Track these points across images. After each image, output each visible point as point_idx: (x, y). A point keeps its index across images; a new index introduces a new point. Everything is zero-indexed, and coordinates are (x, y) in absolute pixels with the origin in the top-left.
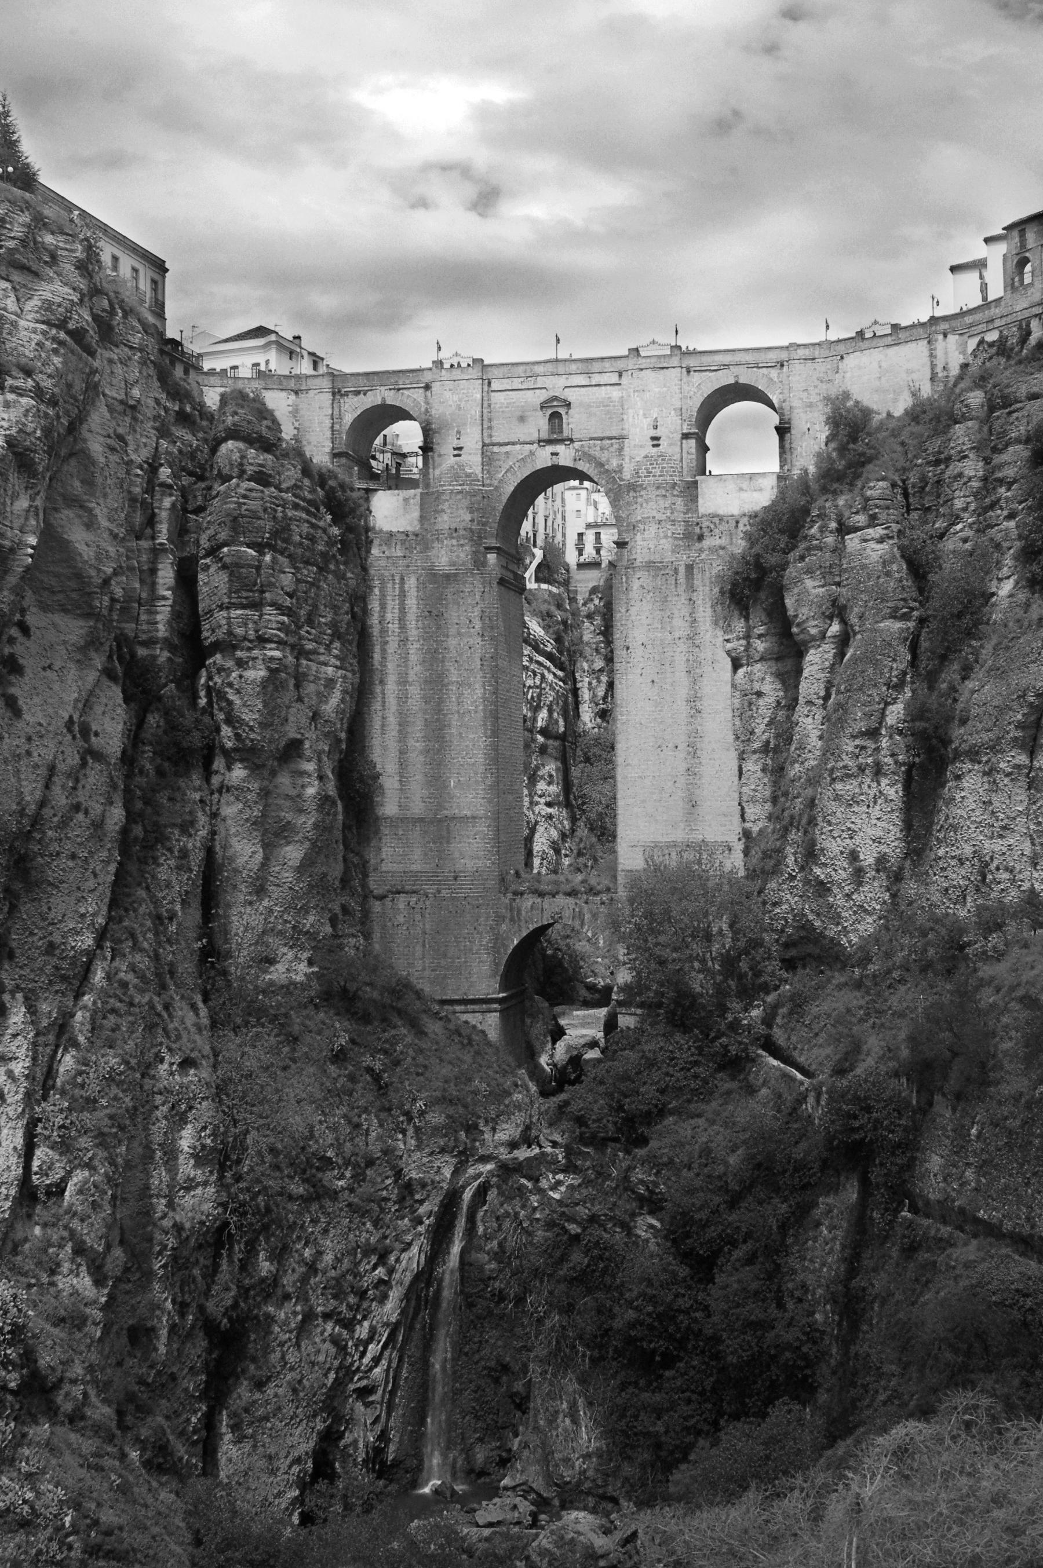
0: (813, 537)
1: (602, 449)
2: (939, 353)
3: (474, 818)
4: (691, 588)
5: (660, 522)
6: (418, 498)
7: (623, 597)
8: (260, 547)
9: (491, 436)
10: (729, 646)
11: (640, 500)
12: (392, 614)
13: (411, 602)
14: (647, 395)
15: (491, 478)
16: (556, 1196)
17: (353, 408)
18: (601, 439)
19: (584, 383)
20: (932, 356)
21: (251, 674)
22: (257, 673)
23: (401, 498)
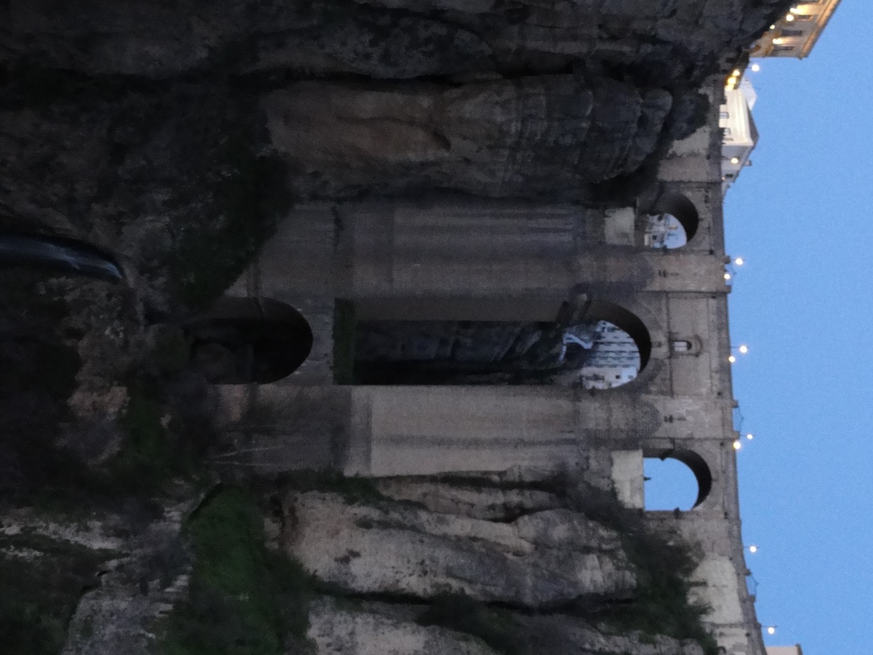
0: (594, 530)
1: (664, 380)
3: (391, 281)
4: (558, 443)
5: (608, 420)
6: (628, 244)
8: (593, 118)
10: (516, 470)
11: (625, 406)
12: (543, 223)
13: (551, 239)
14: (703, 414)
16: (107, 332)
17: (695, 197)
18: (671, 379)
20: (731, 626)
21: (498, 110)
22: (499, 117)
23: (628, 231)
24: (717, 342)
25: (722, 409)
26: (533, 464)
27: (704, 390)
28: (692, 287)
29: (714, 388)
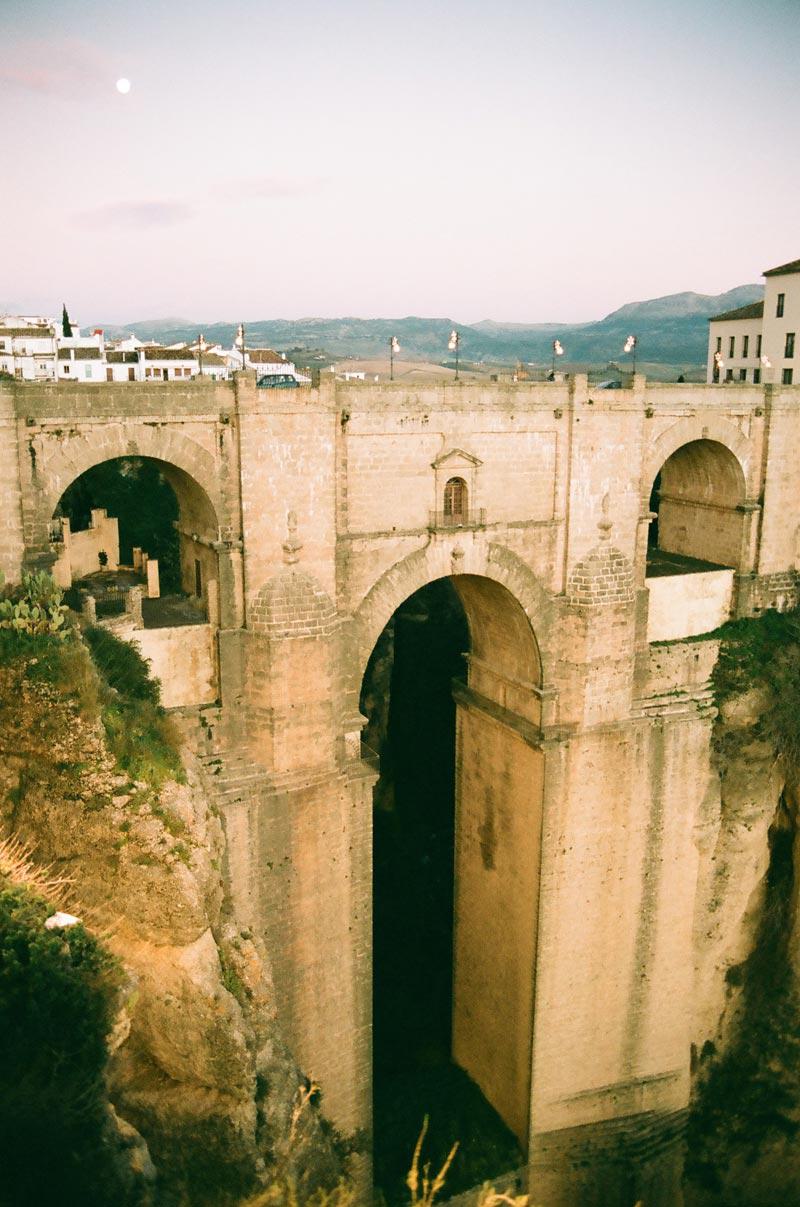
1: (524, 541)
5: (618, 662)
7: (561, 781)
9: (346, 523)
11: (590, 632)
15: (347, 600)
18: (525, 525)
19: (502, 428)
24: (450, 415)
28: (320, 477)
29: (546, 426)
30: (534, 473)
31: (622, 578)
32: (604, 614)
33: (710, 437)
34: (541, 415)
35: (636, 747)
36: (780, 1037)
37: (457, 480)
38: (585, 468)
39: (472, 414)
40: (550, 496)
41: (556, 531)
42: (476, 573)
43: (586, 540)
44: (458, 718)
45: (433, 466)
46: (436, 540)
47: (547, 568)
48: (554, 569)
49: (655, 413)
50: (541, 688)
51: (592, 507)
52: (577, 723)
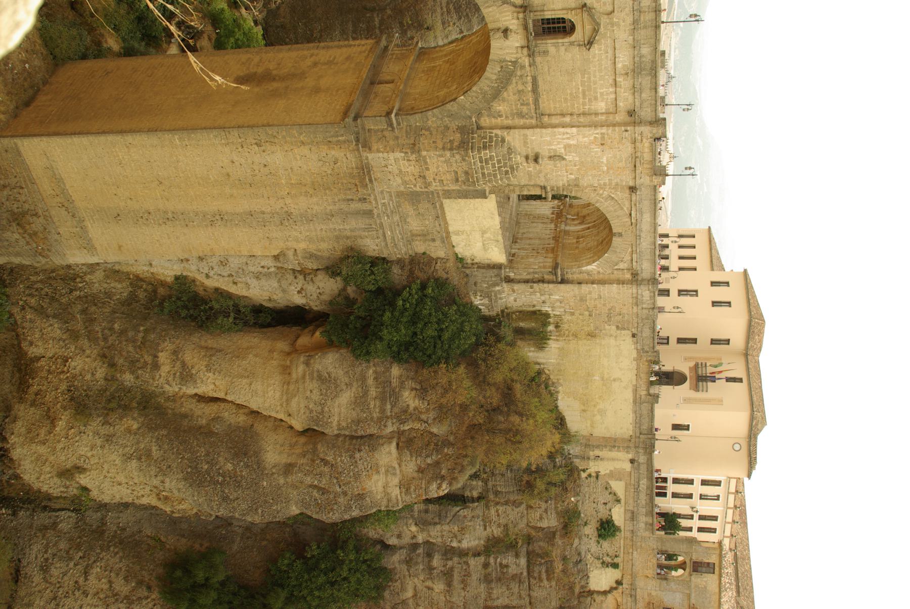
1: (520, 92)
2: (614, 454)
5: (424, 177)
10: (290, 254)
11: (448, 154)
14: (597, 149)
19: (619, 65)
24: (629, 20)
25: (634, 142)
26: (312, 248)
27: (601, 106)
29: (621, 104)
30: (581, 96)
31: (495, 176)
32: (464, 164)
33: (614, 239)
34: (630, 98)
35: (354, 198)
36: (142, 328)
37: (573, 28)
38: (586, 139)
39: (631, 38)
40: (562, 110)
41: (532, 118)
42: (492, 51)
43: (525, 143)
44: (363, 42)
45: (585, 5)
46: (518, 12)
47: (500, 112)
48: (499, 119)
49: (634, 195)
50: (396, 115)
51: (553, 147)
52: (370, 149)
